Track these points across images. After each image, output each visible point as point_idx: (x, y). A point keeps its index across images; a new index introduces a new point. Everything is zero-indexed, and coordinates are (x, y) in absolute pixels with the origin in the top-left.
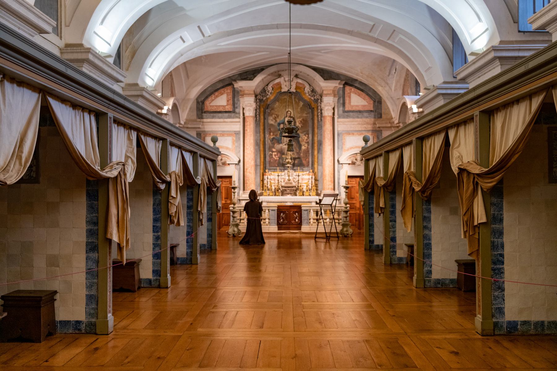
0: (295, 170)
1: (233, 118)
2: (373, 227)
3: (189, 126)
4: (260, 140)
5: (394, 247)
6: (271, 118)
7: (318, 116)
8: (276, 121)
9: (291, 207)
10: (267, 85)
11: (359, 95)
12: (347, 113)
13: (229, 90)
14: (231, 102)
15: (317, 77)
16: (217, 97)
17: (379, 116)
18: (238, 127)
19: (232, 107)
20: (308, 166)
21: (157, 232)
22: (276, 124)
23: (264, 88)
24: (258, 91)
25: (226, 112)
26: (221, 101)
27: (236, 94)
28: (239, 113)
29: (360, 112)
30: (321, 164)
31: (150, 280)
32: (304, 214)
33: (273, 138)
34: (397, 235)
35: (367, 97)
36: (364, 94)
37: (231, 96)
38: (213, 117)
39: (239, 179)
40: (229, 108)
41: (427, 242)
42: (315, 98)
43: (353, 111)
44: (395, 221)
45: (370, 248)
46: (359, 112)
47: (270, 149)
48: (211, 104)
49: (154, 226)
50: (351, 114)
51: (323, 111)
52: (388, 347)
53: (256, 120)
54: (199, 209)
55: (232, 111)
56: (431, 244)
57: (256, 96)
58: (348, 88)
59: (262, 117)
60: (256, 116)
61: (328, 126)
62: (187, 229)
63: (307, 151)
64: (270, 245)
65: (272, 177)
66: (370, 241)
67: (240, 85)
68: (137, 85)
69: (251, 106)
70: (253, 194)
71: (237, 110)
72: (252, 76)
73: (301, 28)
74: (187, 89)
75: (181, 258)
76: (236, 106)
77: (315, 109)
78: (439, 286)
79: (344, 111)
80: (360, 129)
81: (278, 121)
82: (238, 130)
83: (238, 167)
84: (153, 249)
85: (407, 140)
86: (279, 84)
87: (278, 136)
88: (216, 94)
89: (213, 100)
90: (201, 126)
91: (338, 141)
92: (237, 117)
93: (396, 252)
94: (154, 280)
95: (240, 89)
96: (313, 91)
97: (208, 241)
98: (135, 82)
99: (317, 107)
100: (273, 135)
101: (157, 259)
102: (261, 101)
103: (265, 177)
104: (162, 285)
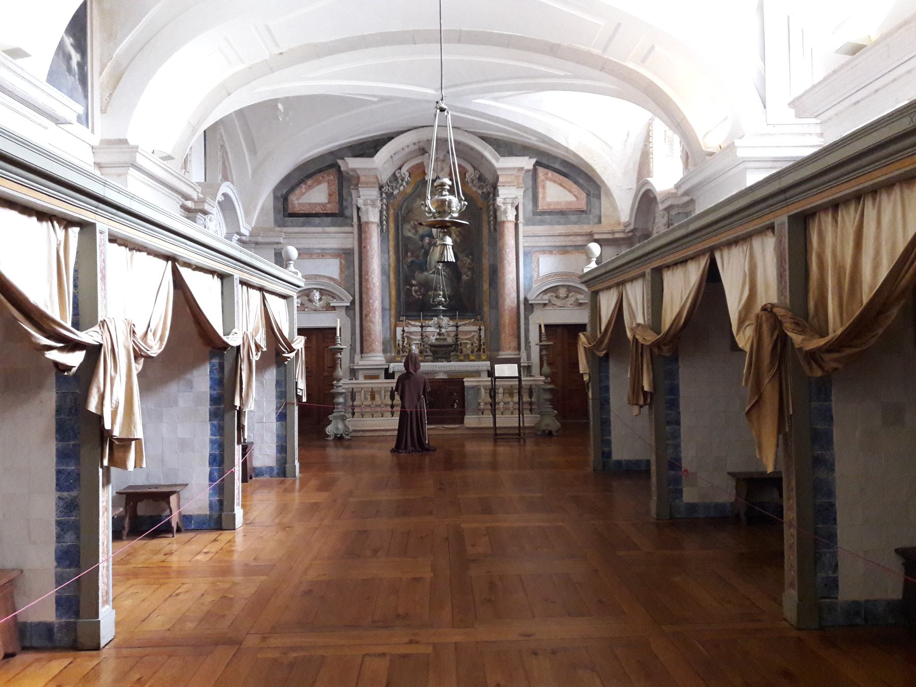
0: (452, 318)
1: (341, 226)
2: (609, 425)
3: (260, 239)
4: (389, 265)
5: (677, 481)
6: (407, 227)
7: (489, 222)
8: (417, 231)
10: (400, 168)
11: (561, 185)
12: (540, 215)
14: (336, 197)
15: (488, 153)
16: (310, 187)
17: (596, 220)
18: (351, 242)
19: (337, 206)
21: (69, 489)
22: (417, 237)
23: (394, 175)
24: (385, 177)
25: (327, 215)
26: (317, 195)
27: (345, 184)
28: (352, 218)
29: (562, 213)
31: (47, 629)
32: (469, 396)
33: (412, 262)
34: (683, 455)
35: (575, 188)
37: (335, 187)
38: (303, 225)
40: (333, 208)
41: (825, 500)
42: (485, 190)
43: (551, 213)
44: (678, 423)
45: (604, 466)
46: (561, 214)
47: (407, 282)
48: (302, 201)
49: (59, 472)
50: (548, 217)
51: (498, 213)
52: (600, 601)
53: (382, 231)
54: (237, 403)
55: (340, 213)
56: (833, 505)
57: (381, 188)
58: (541, 171)
59: (392, 225)
60: (381, 222)
62: (212, 449)
65: (413, 329)
66: (603, 453)
67: (353, 164)
68: (124, 142)
69: (373, 204)
72: (372, 150)
73: (459, 41)
74: (254, 172)
75: (199, 516)
76: (345, 203)
77: (484, 209)
78: (859, 621)
79: (535, 213)
80: (564, 244)
82: (350, 246)
83: (352, 312)
84: (59, 537)
85: (766, 221)
87: (421, 258)
88: (309, 182)
89: (304, 194)
90: (282, 240)
91: (525, 265)
92: (346, 225)
93: (681, 492)
94: (61, 626)
95: (351, 173)
96: (481, 178)
97: (278, 460)
98: (122, 138)
99: (488, 207)
100: (412, 254)
101: (69, 566)
102: (390, 195)
103: (399, 330)
104: (83, 640)
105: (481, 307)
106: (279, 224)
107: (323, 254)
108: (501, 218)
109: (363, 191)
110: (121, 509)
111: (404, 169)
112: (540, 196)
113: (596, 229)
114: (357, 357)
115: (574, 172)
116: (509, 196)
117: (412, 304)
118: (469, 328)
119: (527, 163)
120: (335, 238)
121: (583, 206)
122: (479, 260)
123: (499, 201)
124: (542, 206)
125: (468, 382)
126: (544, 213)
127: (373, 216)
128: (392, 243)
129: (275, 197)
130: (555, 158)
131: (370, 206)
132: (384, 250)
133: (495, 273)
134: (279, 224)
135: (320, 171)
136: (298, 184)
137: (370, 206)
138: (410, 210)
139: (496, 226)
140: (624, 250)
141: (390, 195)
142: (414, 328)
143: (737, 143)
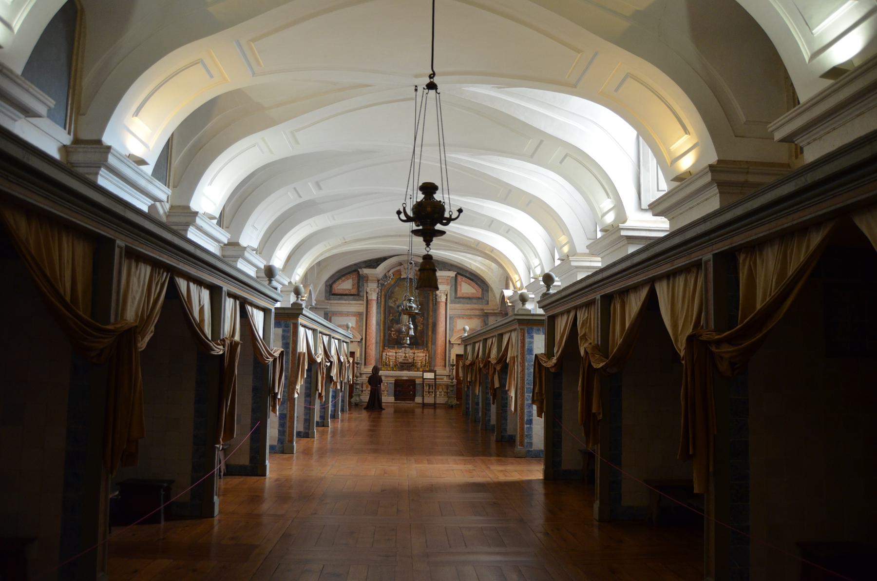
0: (411, 349)
9: (406, 380)
12: (458, 299)
13: (354, 276)
16: (343, 281)
18: (362, 309)
20: (423, 345)
24: (380, 276)
26: (346, 285)
27: (361, 280)
29: (469, 298)
30: (434, 342)
35: (476, 286)
37: (356, 281)
38: (339, 299)
39: (361, 355)
40: (354, 291)
43: (463, 298)
46: (469, 299)
47: (389, 329)
55: (357, 294)
58: (459, 277)
59: (383, 300)
61: (442, 311)
63: (422, 332)
64: (388, 412)
67: (366, 271)
70: (376, 370)
71: (361, 294)
79: (456, 298)
81: (397, 303)
102: (382, 285)
103: (384, 354)
105: (427, 344)
106: (327, 298)
107: (348, 314)
108: (439, 300)
109: (369, 284)
110: (117, 493)
111: (390, 273)
113: (485, 307)
114: (363, 367)
115: (474, 278)
116: (443, 289)
118: (420, 355)
119: (452, 274)
120: (356, 306)
122: (428, 321)
124: (459, 295)
125: (418, 381)
126: (460, 298)
127: (373, 296)
128: (382, 309)
129: (326, 286)
130: (467, 271)
131: (372, 291)
132: (378, 313)
133: (435, 325)
134: (327, 298)
135: (349, 273)
136: (337, 279)
137: (372, 291)
138: (392, 293)
139: (436, 303)
140: (499, 319)
141: (382, 285)
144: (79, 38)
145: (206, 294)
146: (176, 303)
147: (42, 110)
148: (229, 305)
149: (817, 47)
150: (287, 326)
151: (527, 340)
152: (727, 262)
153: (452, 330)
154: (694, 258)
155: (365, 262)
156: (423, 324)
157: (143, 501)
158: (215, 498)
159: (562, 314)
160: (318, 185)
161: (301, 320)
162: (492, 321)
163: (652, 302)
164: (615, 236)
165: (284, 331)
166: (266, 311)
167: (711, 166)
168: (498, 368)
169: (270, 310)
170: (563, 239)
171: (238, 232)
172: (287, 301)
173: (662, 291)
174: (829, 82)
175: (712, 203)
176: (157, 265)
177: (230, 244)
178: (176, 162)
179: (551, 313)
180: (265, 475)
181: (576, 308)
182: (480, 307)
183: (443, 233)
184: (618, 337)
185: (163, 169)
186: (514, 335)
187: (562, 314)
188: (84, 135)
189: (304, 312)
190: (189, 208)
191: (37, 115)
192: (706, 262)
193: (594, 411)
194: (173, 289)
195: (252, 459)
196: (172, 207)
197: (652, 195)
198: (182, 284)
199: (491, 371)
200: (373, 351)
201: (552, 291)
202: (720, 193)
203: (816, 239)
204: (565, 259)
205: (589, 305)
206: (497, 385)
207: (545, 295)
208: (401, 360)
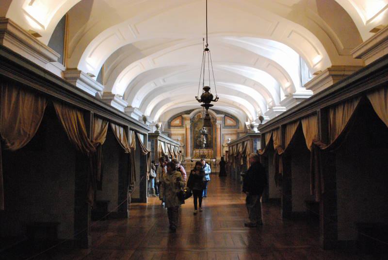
10: (195, 115)
12: (226, 127)
13: (180, 118)
18: (184, 132)
26: (177, 122)
27: (183, 119)
30: (216, 145)
35: (234, 121)
36: (232, 120)
40: (180, 125)
46: (230, 126)
47: (196, 140)
55: (181, 126)
58: (226, 117)
61: (219, 132)
63: (210, 141)
67: (185, 116)
79: (225, 126)
81: (199, 129)
86: (200, 115)
96: (213, 118)
102: (192, 121)
103: (194, 151)
111: (196, 116)
112: (226, 122)
115: (232, 117)
116: (219, 123)
117: (197, 145)
118: (210, 151)
119: (223, 116)
121: (235, 125)
123: (217, 123)
124: (226, 124)
127: (188, 126)
130: (229, 114)
133: (216, 138)
135: (178, 117)
137: (188, 124)
139: (216, 128)
140: (244, 135)
142: (197, 151)
143: (273, 108)
144: (67, 27)
145: (122, 129)
146: (111, 133)
147: (56, 59)
148: (131, 134)
149: (368, 19)
150: (153, 141)
151: (254, 144)
152: (325, 112)
153: (224, 140)
154: (314, 110)
155: (185, 112)
156: (211, 138)
157: (101, 212)
158: (128, 210)
159: (267, 132)
160: (164, 81)
161: (158, 138)
162: (241, 135)
163: (300, 128)
164: (290, 99)
165: (152, 143)
166: (145, 135)
167: (328, 69)
168: (243, 155)
169: (146, 135)
170: (270, 100)
171: (131, 101)
172: (154, 130)
173: (304, 124)
174: (373, 34)
175: (330, 83)
176: (104, 119)
177: (128, 107)
178: (105, 74)
179: (264, 132)
180: (146, 202)
181: (273, 130)
182: (235, 129)
183: (212, 105)
184: (288, 142)
185: (100, 78)
186: (249, 142)
187: (267, 132)
188: (70, 67)
189: (160, 135)
190: (111, 93)
191: (54, 61)
192: (318, 112)
193: (280, 172)
194: (110, 128)
195: (141, 196)
196: (104, 93)
197: (305, 82)
198: (113, 126)
199: (239, 156)
200: (189, 151)
201: (263, 123)
202: (333, 79)
203: (356, 104)
204: (271, 108)
205: (277, 129)
206: (242, 164)
207: (260, 125)
208: (201, 154)
